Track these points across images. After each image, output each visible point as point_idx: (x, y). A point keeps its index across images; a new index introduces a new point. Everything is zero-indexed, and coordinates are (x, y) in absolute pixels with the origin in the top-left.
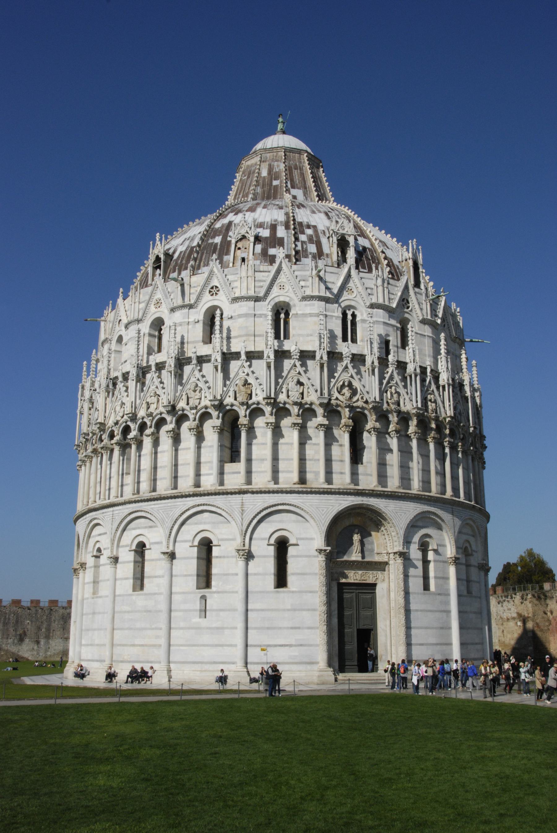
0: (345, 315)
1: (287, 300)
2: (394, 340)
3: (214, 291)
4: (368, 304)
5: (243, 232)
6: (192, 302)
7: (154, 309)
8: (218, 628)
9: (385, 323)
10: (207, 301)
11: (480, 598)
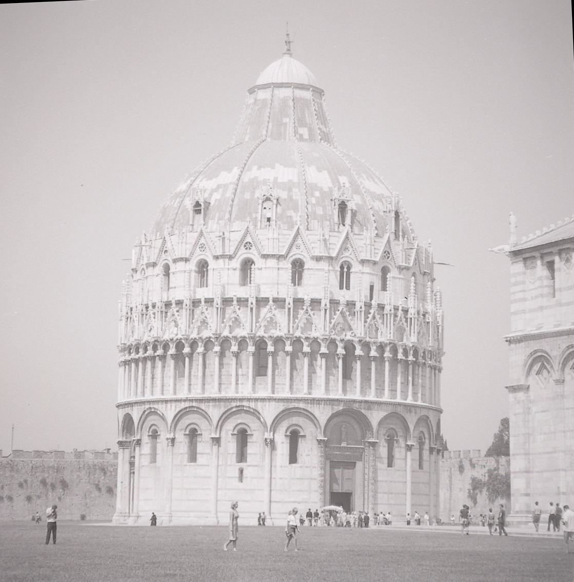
0: (342, 267)
1: (301, 257)
2: (378, 286)
3: (248, 246)
4: (359, 260)
5: (268, 195)
6: (231, 253)
7: (199, 251)
8: (251, 490)
9: (370, 274)
10: (243, 254)
11: (430, 473)
